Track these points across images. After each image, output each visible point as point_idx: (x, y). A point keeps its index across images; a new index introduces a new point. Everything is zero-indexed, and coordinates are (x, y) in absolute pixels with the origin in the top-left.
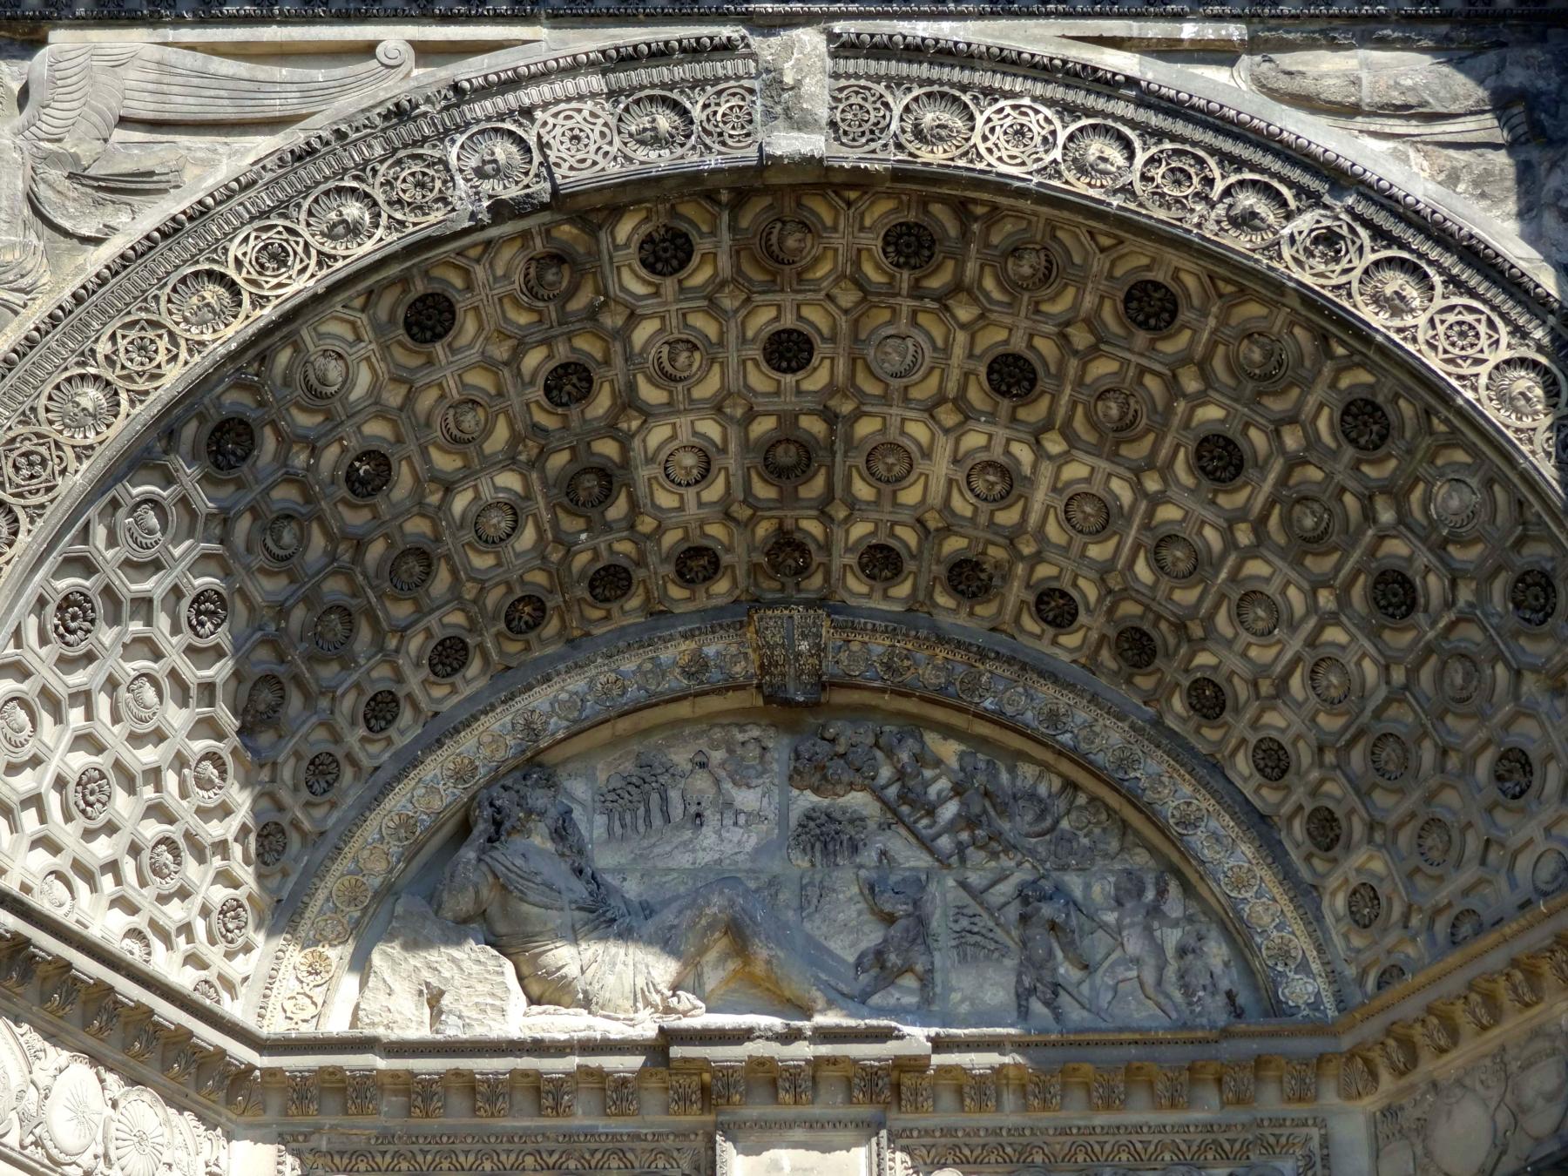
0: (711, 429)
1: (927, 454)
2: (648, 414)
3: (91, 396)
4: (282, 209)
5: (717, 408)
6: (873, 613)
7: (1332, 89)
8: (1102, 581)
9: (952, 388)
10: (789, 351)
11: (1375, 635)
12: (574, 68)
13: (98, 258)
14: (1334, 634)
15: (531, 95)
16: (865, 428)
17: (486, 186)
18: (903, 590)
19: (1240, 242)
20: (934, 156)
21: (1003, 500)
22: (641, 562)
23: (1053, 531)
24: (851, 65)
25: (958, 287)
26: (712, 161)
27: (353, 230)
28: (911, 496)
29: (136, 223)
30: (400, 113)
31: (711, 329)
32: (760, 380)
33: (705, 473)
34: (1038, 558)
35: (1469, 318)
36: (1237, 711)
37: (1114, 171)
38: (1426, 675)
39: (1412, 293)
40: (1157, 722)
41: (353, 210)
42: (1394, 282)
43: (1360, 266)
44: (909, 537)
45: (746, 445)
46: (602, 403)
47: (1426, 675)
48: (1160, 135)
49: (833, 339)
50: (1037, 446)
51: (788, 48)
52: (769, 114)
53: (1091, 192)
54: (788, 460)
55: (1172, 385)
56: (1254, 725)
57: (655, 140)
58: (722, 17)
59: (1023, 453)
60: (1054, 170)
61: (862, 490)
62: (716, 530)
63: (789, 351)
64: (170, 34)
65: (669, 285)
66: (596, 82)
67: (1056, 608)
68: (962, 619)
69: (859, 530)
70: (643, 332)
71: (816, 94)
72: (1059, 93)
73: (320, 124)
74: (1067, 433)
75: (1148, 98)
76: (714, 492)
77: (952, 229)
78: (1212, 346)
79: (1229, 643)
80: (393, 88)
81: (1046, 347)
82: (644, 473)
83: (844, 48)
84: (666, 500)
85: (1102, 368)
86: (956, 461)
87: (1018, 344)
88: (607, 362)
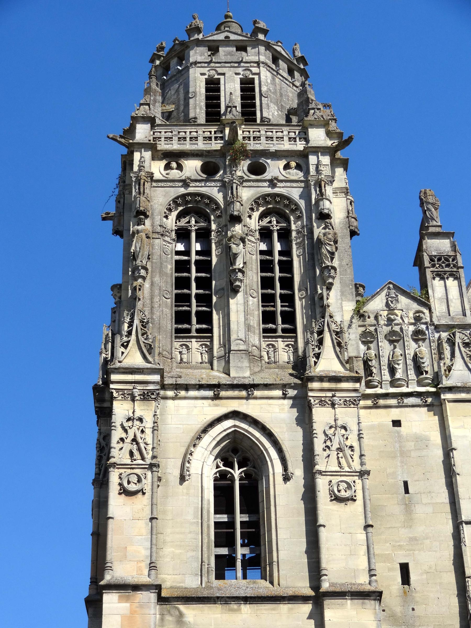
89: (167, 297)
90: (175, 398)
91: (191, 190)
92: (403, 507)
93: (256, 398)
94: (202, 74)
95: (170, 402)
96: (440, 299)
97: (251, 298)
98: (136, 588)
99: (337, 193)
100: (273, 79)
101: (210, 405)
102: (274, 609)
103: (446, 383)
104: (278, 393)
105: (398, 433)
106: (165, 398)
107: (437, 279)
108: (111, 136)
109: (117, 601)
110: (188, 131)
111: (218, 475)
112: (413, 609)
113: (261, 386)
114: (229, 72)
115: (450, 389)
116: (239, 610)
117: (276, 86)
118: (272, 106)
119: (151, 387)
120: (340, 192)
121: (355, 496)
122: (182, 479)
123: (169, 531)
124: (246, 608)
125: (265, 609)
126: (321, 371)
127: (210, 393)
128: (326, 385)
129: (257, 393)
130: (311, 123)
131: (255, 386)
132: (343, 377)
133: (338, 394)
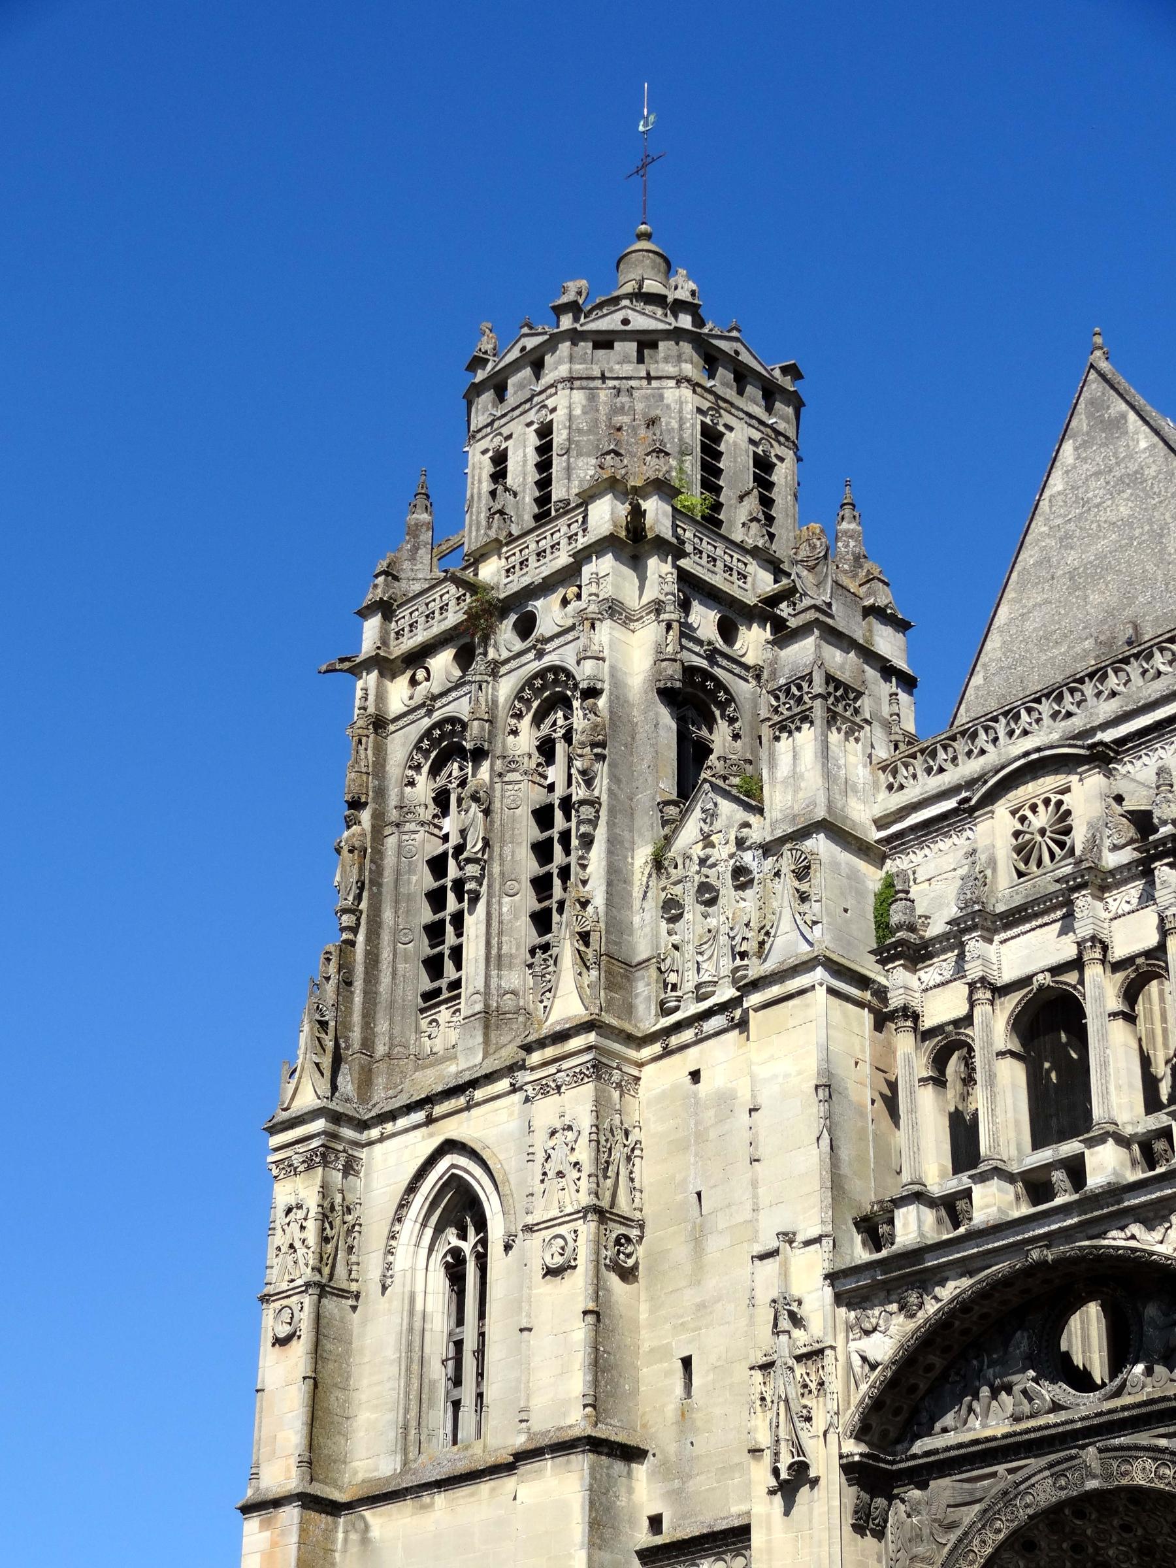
4: (983, 1527)
10: (1126, 1528)
12: (1041, 1471)
15: (1033, 1480)
24: (1103, 1455)
26: (1075, 1493)
29: (953, 1537)
30: (1006, 1493)
53: (1162, 1486)
57: (1062, 1488)
58: (1071, 1448)
60: (1151, 1481)
64: (954, 1478)
66: (1047, 1473)
71: (1095, 1466)
72: (1152, 1454)
80: (1002, 1485)
83: (1100, 1451)
89: (406, 940)
90: (382, 1139)
91: (437, 716)
92: (693, 1244)
93: (478, 1104)
94: (484, 452)
95: (378, 1147)
96: (784, 782)
97: (506, 899)
98: (277, 1503)
99: (642, 617)
100: (592, 398)
101: (423, 1138)
102: (472, 1495)
103: (755, 969)
104: (503, 1085)
105: (695, 1095)
106: (370, 1143)
107: (784, 735)
108: (324, 668)
109: (257, 1530)
110: (437, 596)
111: (449, 1259)
112: (692, 1443)
113: (482, 1081)
114: (516, 427)
115: (756, 985)
116: (432, 1504)
117: (597, 410)
118: (580, 464)
119: (315, 1143)
120: (647, 614)
121: (575, 1259)
122: (384, 1288)
123: (365, 1382)
124: (440, 1499)
125: (463, 1497)
126: (558, 1022)
127: (419, 1116)
128: (550, 1052)
129: (479, 1094)
130: (590, 493)
131: (474, 1084)
132: (569, 1029)
133: (565, 1065)
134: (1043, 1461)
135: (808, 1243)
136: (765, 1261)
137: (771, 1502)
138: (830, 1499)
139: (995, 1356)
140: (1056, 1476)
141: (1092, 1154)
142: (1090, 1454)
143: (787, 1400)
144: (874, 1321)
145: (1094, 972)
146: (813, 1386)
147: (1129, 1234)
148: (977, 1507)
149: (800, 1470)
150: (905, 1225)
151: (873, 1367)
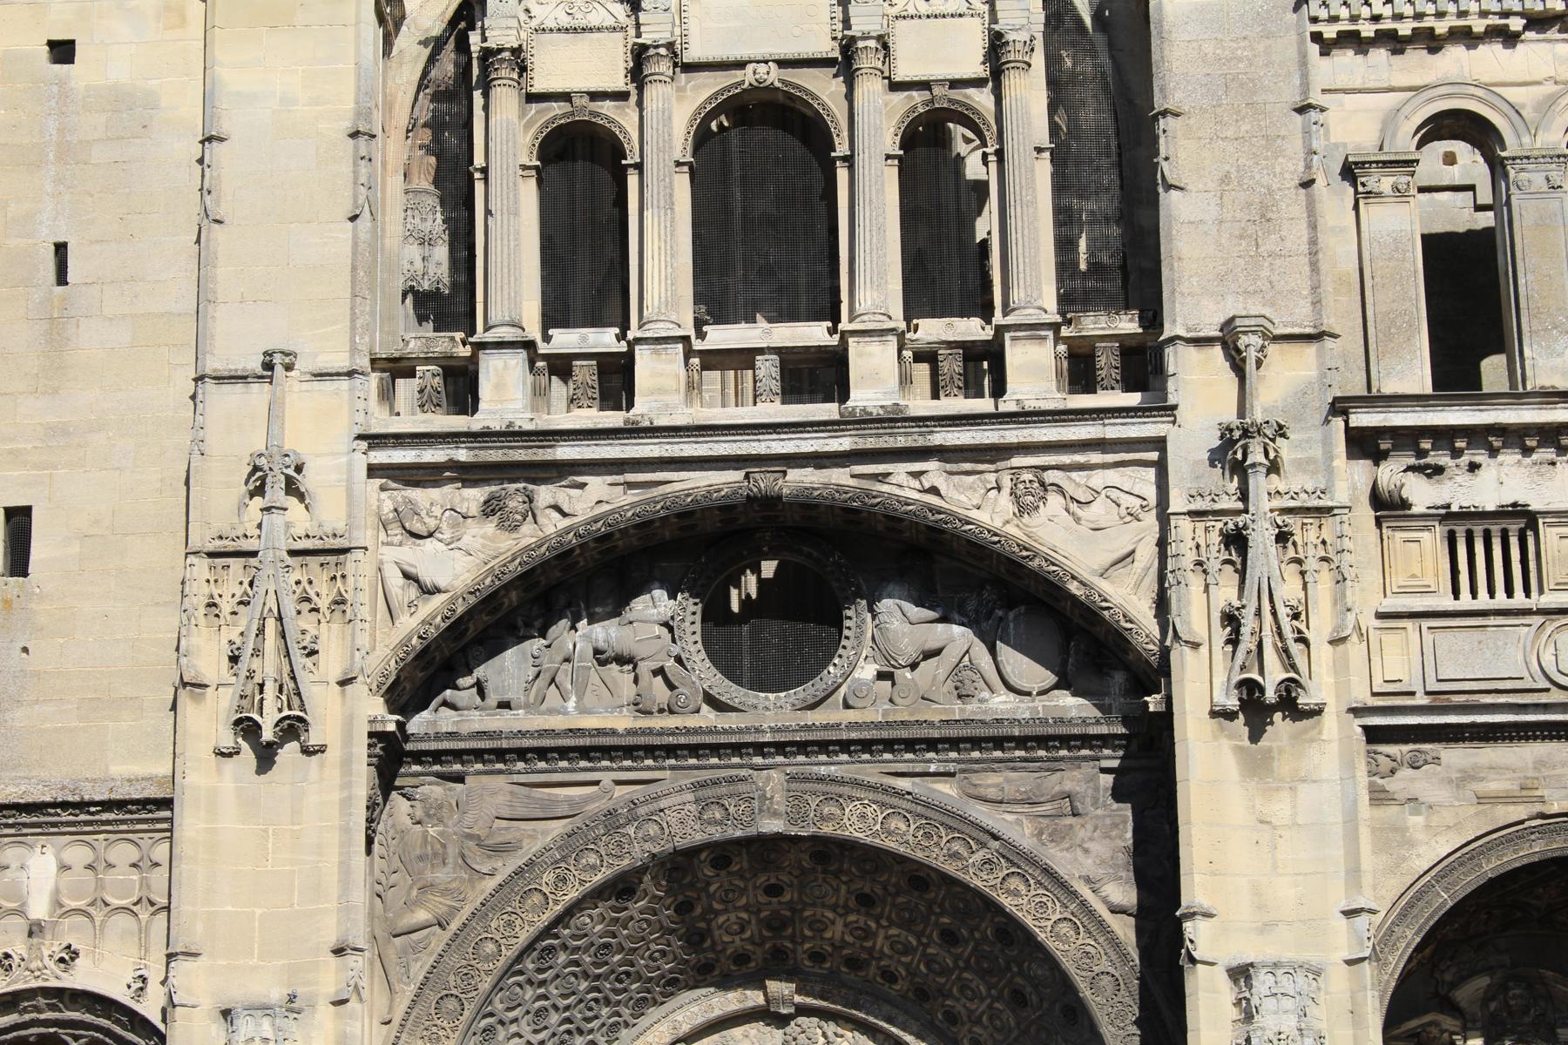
0: (745, 916)
1: (833, 923)
2: (717, 913)
3: (490, 947)
4: (564, 858)
5: (746, 908)
6: (815, 974)
7: (992, 793)
8: (907, 970)
9: (841, 902)
10: (774, 890)
11: (1013, 1011)
13: (490, 884)
14: (997, 1005)
15: (663, 804)
16: (807, 913)
17: (648, 846)
18: (828, 965)
19: (950, 868)
20: (827, 829)
21: (866, 938)
22: (718, 961)
23: (886, 950)
24: (793, 786)
25: (840, 871)
26: (739, 833)
27: (593, 867)
28: (828, 935)
29: (506, 867)
31: (742, 884)
32: (763, 899)
33: (742, 930)
34: (880, 959)
35: (1044, 899)
36: (963, 1024)
37: (899, 836)
38: (1033, 1029)
39: (1022, 888)
40: (932, 1023)
41: (592, 859)
42: (1014, 883)
43: (1001, 875)
44: (829, 949)
45: (760, 921)
46: (698, 910)
47: (1033, 1029)
48: (920, 816)
49: (791, 886)
50: (877, 922)
51: (769, 779)
52: (761, 811)
54: (776, 924)
55: (930, 908)
56: (970, 1031)
59: (873, 925)
60: (876, 834)
61: (808, 933)
62: (749, 947)
63: (774, 890)
65: (723, 873)
67: (890, 977)
68: (852, 976)
69: (807, 946)
70: (712, 889)
71: (779, 801)
72: (880, 797)
73: (578, 821)
74: (889, 919)
75: (916, 801)
76: (748, 934)
77: (837, 851)
78: (944, 899)
79: (958, 1000)
81: (879, 891)
82: (717, 933)
83: (793, 778)
84: (726, 938)
85: (900, 900)
86: (846, 925)
87: (867, 890)
88: (699, 898)
134: (687, 779)
135: (320, 376)
136: (226, 388)
137: (219, 771)
138: (332, 781)
139: (599, 610)
140: (704, 805)
141: (860, 355)
142: (773, 780)
143: (280, 619)
144: (432, 523)
145: (870, 89)
146: (323, 603)
147: (927, 486)
148: (558, 828)
149: (292, 728)
150: (499, 387)
151: (429, 591)
